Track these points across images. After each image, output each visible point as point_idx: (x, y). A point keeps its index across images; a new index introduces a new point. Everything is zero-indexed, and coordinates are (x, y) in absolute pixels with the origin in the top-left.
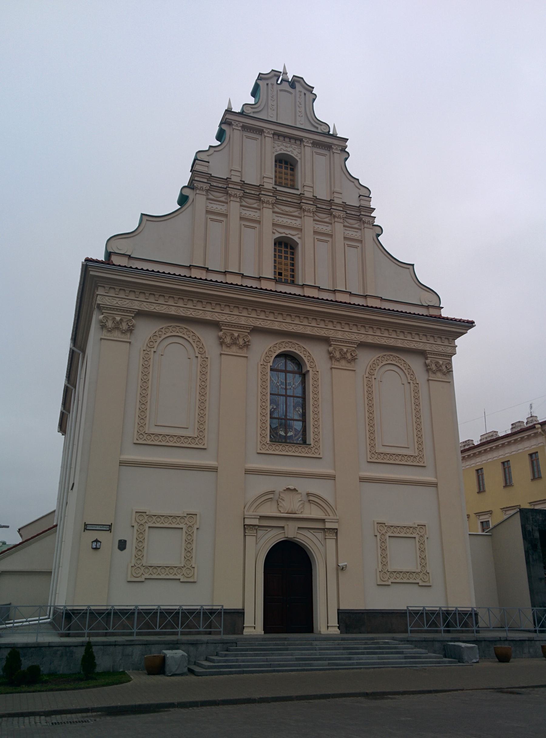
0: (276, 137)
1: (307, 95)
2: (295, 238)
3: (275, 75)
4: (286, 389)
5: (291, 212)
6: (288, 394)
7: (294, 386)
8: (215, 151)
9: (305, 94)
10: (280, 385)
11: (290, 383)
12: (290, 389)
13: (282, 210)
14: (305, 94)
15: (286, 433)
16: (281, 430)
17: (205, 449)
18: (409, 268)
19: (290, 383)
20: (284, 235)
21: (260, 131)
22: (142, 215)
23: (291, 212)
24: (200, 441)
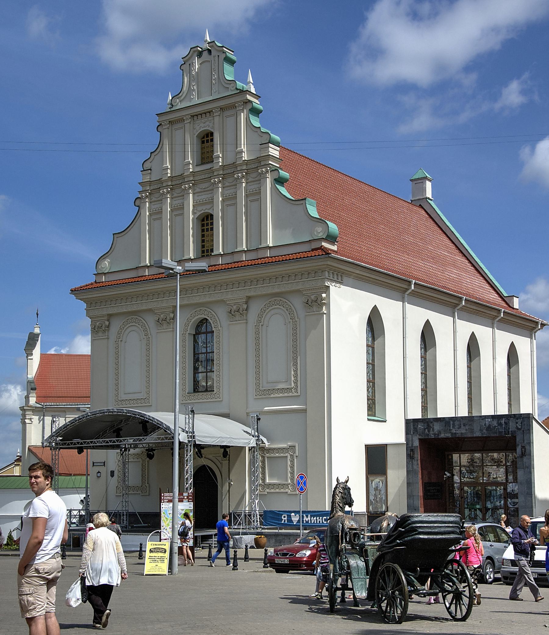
0: (195, 118)
1: (220, 56)
2: (210, 212)
3: (194, 51)
4: (207, 347)
5: (208, 187)
6: (208, 351)
7: (212, 344)
8: (155, 155)
9: (218, 56)
10: (203, 345)
11: (209, 342)
12: (210, 346)
13: (201, 189)
14: (218, 56)
15: (207, 384)
16: (203, 382)
17: (151, 405)
18: (301, 204)
19: (209, 342)
20: (203, 212)
21: (181, 120)
22: (114, 234)
23: (208, 187)
24: (148, 401)
